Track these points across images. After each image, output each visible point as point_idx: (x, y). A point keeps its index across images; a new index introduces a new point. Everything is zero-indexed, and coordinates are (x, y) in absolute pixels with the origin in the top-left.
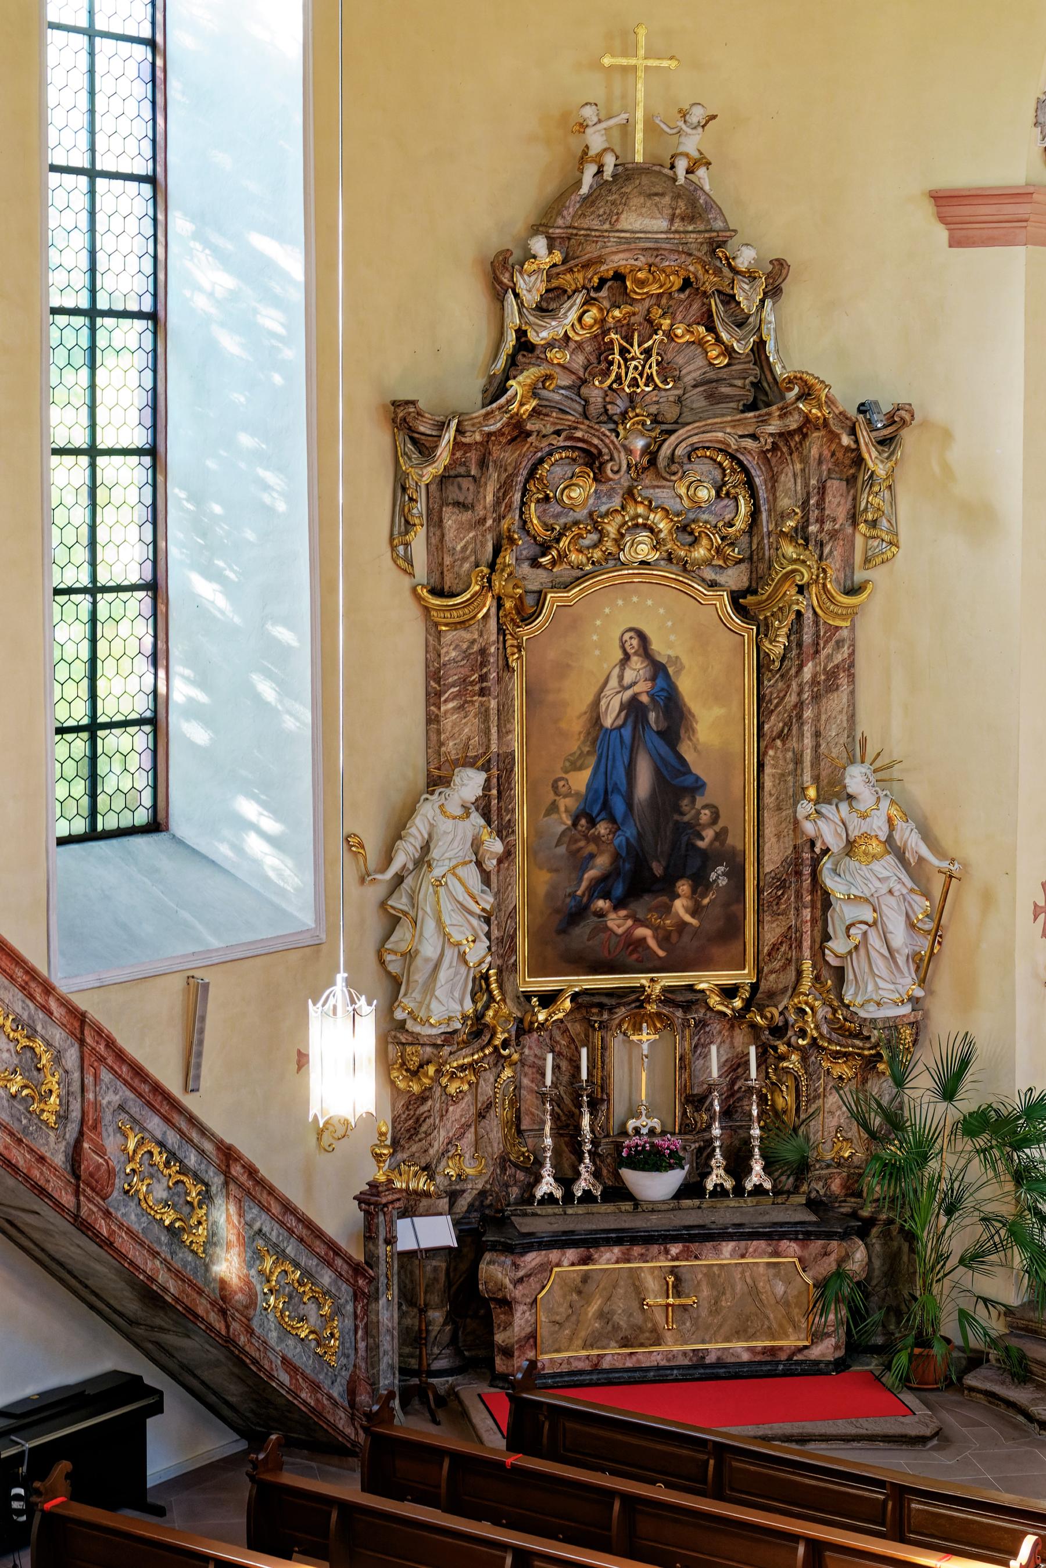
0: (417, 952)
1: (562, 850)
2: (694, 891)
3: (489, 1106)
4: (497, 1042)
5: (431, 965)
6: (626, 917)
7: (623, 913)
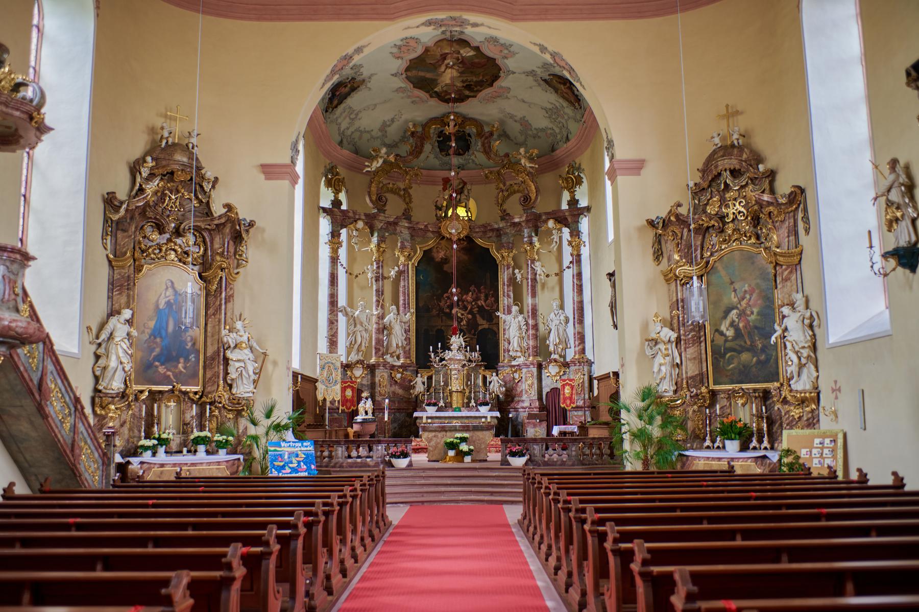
0: (109, 365)
1: (146, 345)
2: (185, 362)
3: (125, 422)
4: (130, 400)
5: (113, 370)
6: (164, 368)
7: (163, 367)
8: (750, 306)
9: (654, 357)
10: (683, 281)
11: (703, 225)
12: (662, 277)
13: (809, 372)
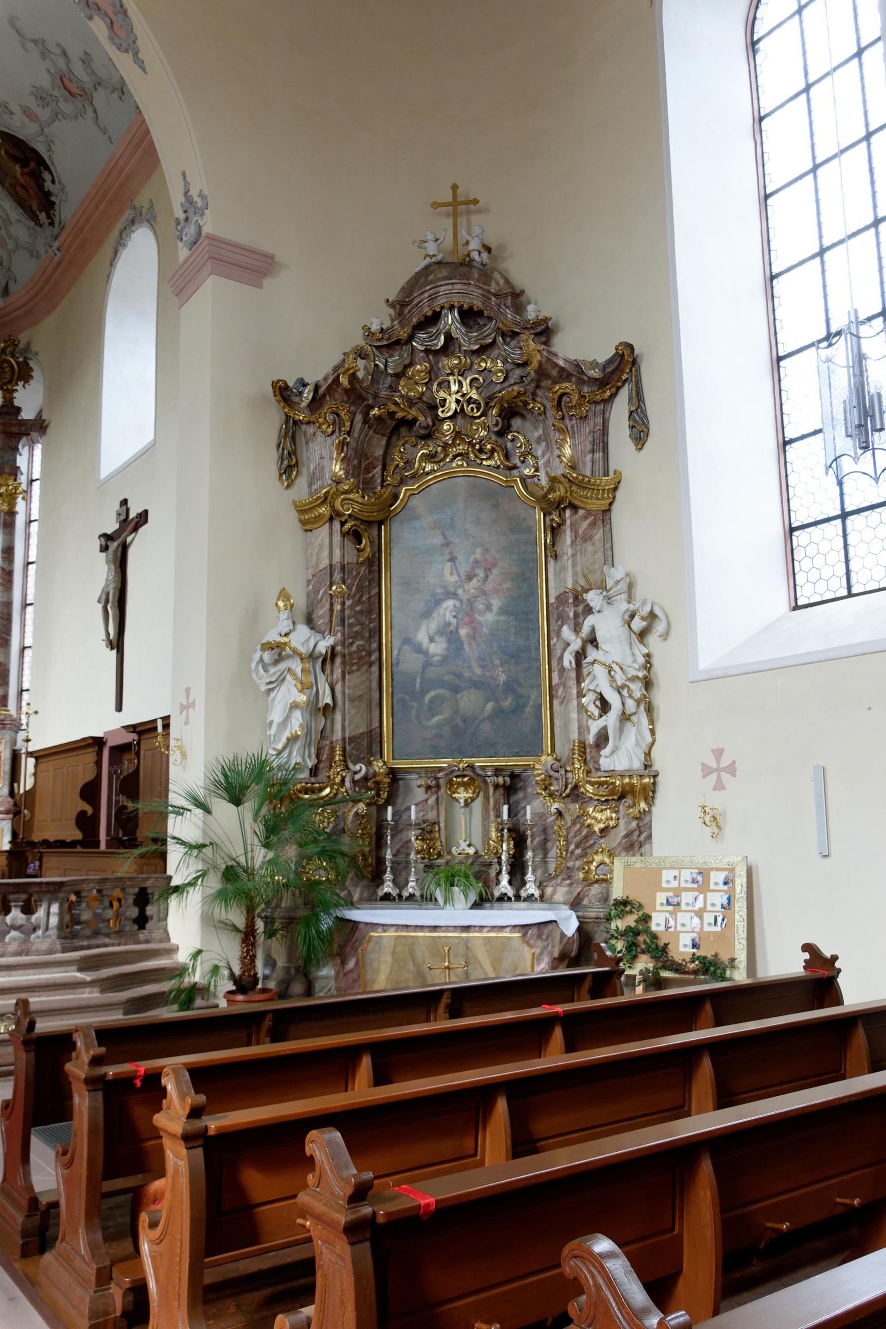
8: (484, 593)
9: (270, 691)
10: (347, 526)
11: (394, 413)
12: (294, 515)
13: (639, 732)
